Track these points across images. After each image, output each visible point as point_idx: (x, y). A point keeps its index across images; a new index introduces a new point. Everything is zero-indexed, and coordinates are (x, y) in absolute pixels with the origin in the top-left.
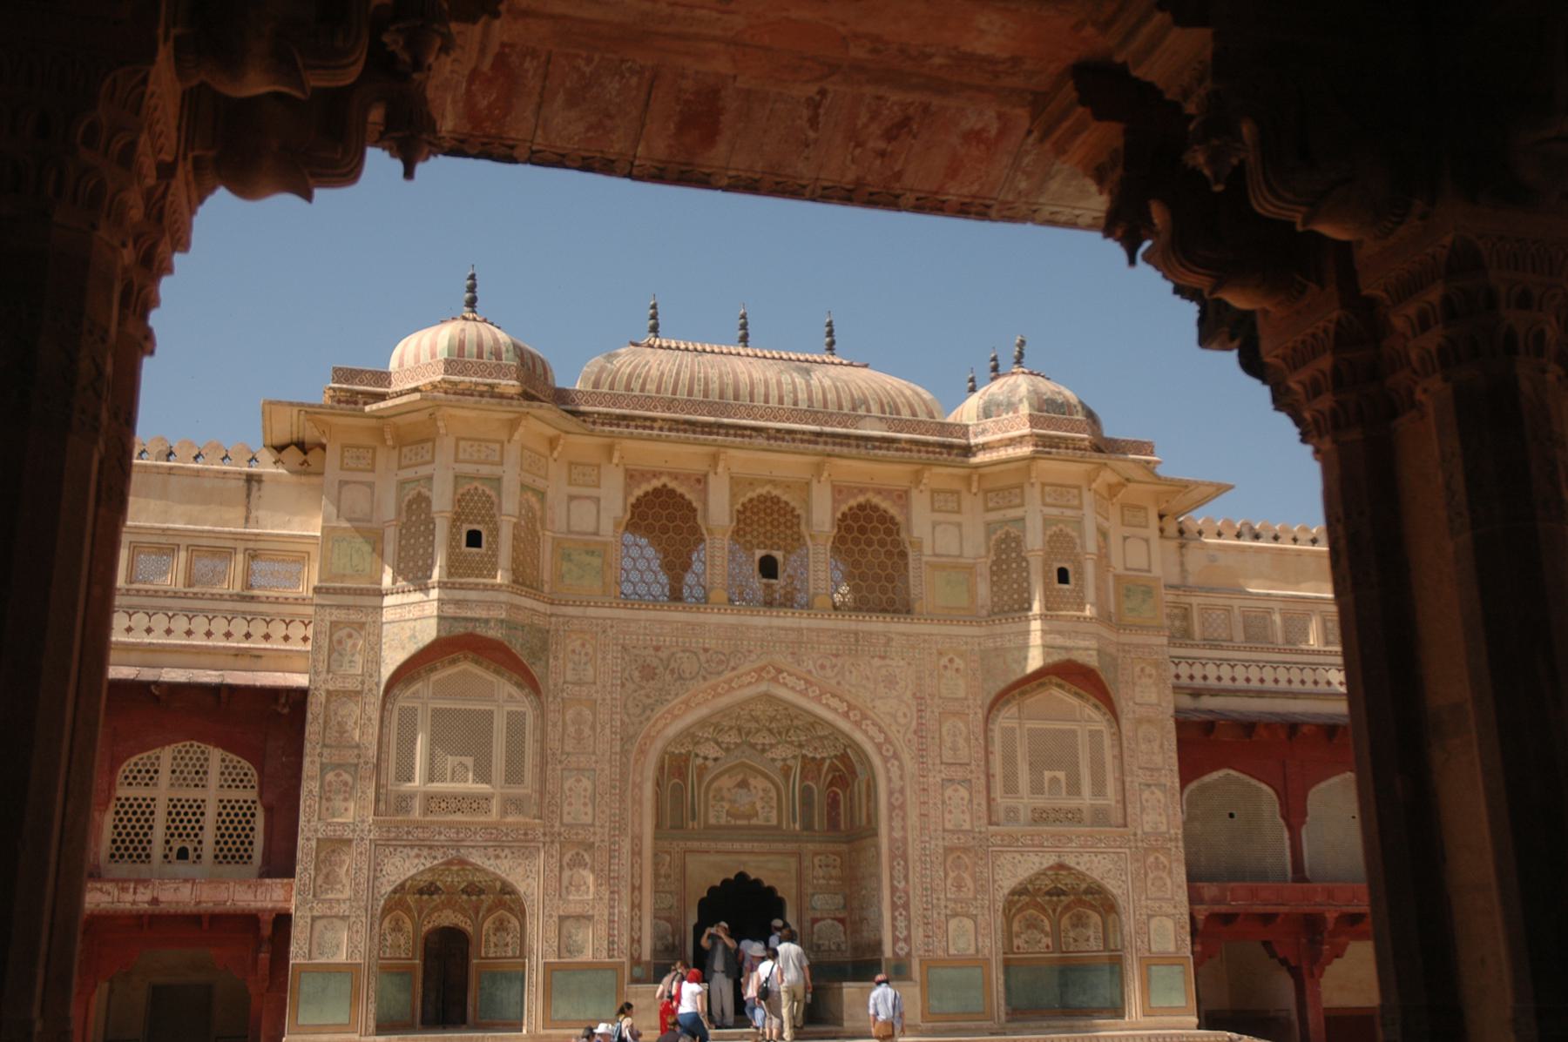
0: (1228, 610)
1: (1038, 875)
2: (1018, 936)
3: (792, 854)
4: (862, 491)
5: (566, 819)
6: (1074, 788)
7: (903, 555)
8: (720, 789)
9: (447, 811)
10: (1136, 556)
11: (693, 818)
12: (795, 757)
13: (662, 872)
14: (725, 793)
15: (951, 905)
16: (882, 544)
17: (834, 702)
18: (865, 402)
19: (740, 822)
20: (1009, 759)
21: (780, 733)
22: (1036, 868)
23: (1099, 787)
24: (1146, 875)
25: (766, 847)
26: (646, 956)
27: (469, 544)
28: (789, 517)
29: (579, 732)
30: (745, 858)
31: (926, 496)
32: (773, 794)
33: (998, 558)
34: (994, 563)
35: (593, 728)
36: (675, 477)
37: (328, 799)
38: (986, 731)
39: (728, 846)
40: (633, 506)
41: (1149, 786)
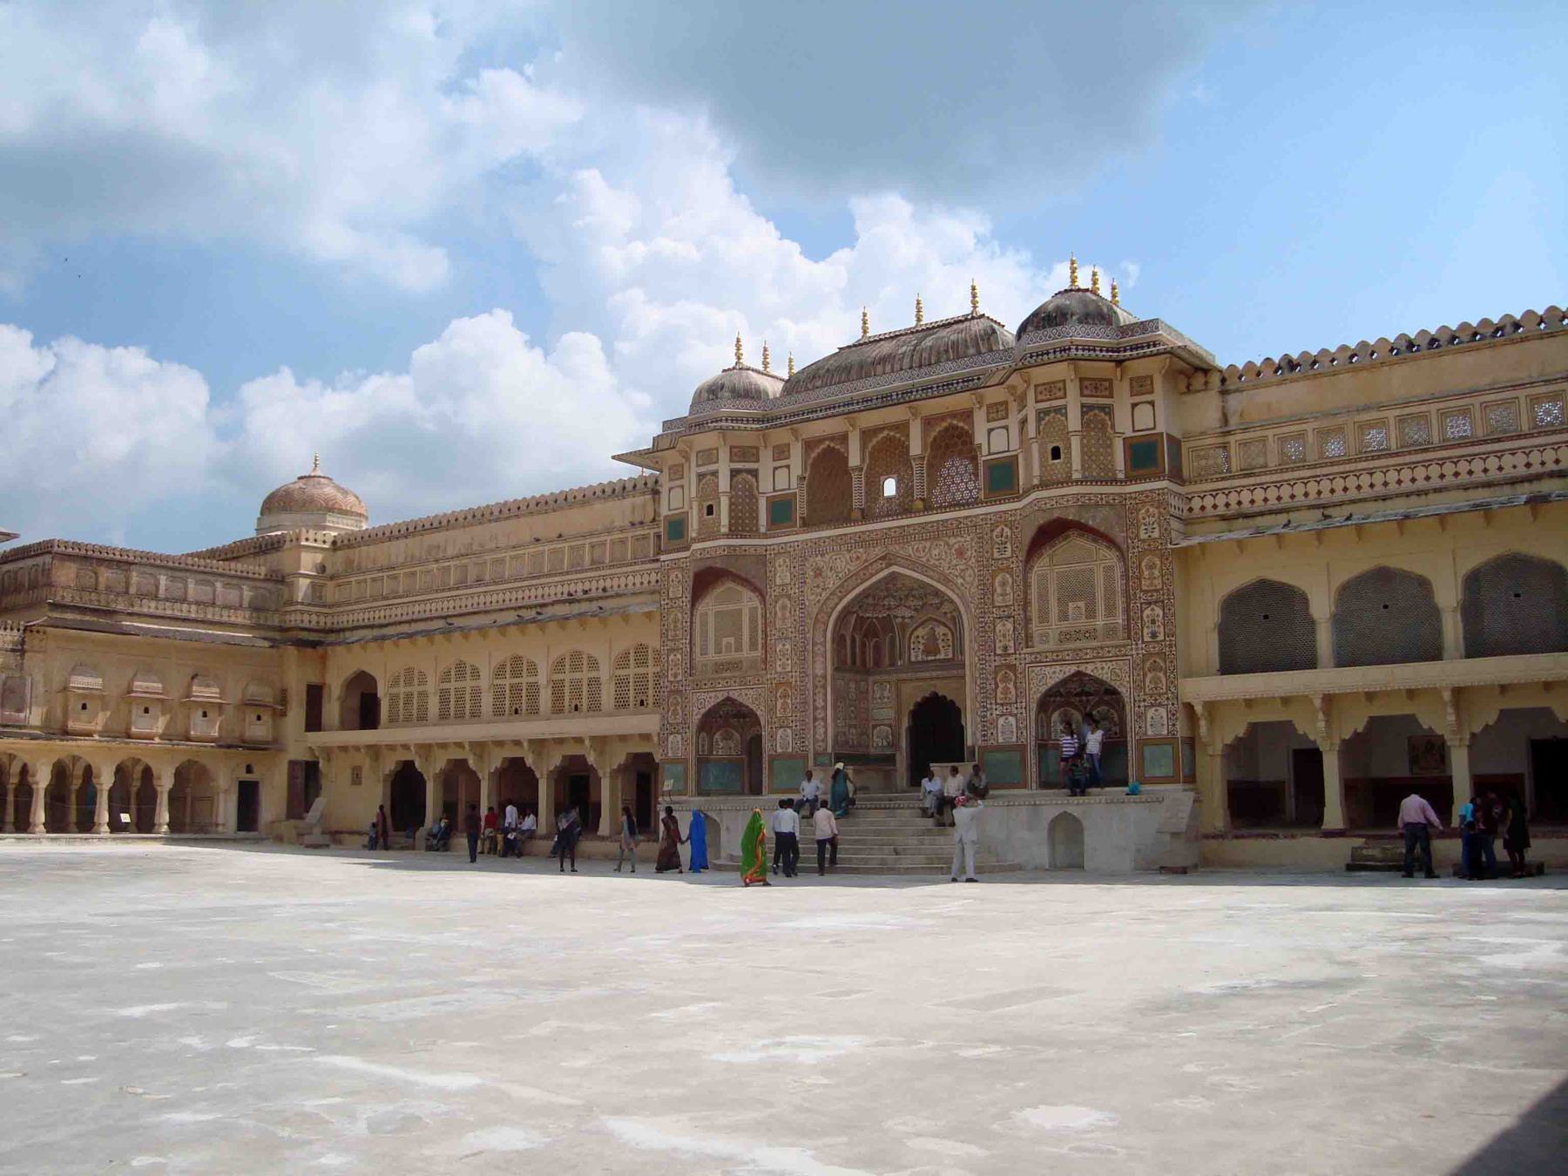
0: (1264, 440)
1: (1064, 682)
4: (942, 418)
6: (1091, 613)
10: (1144, 418)
16: (960, 454)
18: (947, 351)
20: (1043, 598)
22: (1061, 676)
23: (1110, 610)
24: (1145, 675)
25: (945, 673)
36: (832, 438)
38: (1025, 579)
40: (813, 465)
41: (1150, 604)
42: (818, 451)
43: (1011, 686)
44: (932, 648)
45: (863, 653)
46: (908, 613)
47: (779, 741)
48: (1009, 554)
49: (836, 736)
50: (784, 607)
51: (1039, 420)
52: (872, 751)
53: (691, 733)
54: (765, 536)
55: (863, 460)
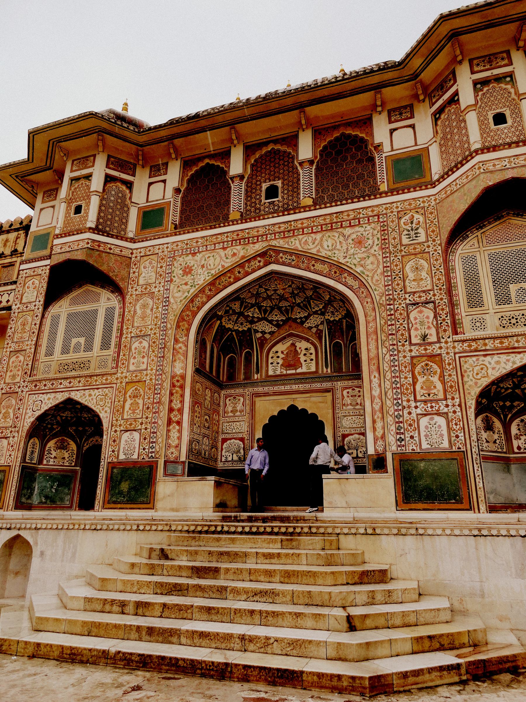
2: (517, 438)
3: (327, 391)
4: (335, 128)
5: (132, 368)
7: (372, 159)
8: (277, 352)
9: (67, 370)
11: (257, 373)
12: (322, 323)
13: (238, 408)
14: (279, 354)
15: (420, 405)
17: (319, 266)
19: (289, 372)
21: (305, 306)
22: (509, 367)
25: (307, 386)
26: (183, 458)
27: (76, 213)
28: (286, 159)
29: (144, 313)
30: (294, 396)
31: (385, 114)
32: (313, 350)
33: (445, 134)
34: (442, 138)
35: (152, 310)
37: (11, 371)
39: (282, 388)
42: (195, 169)
43: (435, 379)
44: (292, 360)
45: (218, 366)
46: (268, 328)
47: (122, 446)
48: (422, 238)
49: (191, 442)
50: (144, 306)
51: (476, 90)
52: (220, 465)
53: (18, 438)
54: (133, 240)
55: (245, 169)
